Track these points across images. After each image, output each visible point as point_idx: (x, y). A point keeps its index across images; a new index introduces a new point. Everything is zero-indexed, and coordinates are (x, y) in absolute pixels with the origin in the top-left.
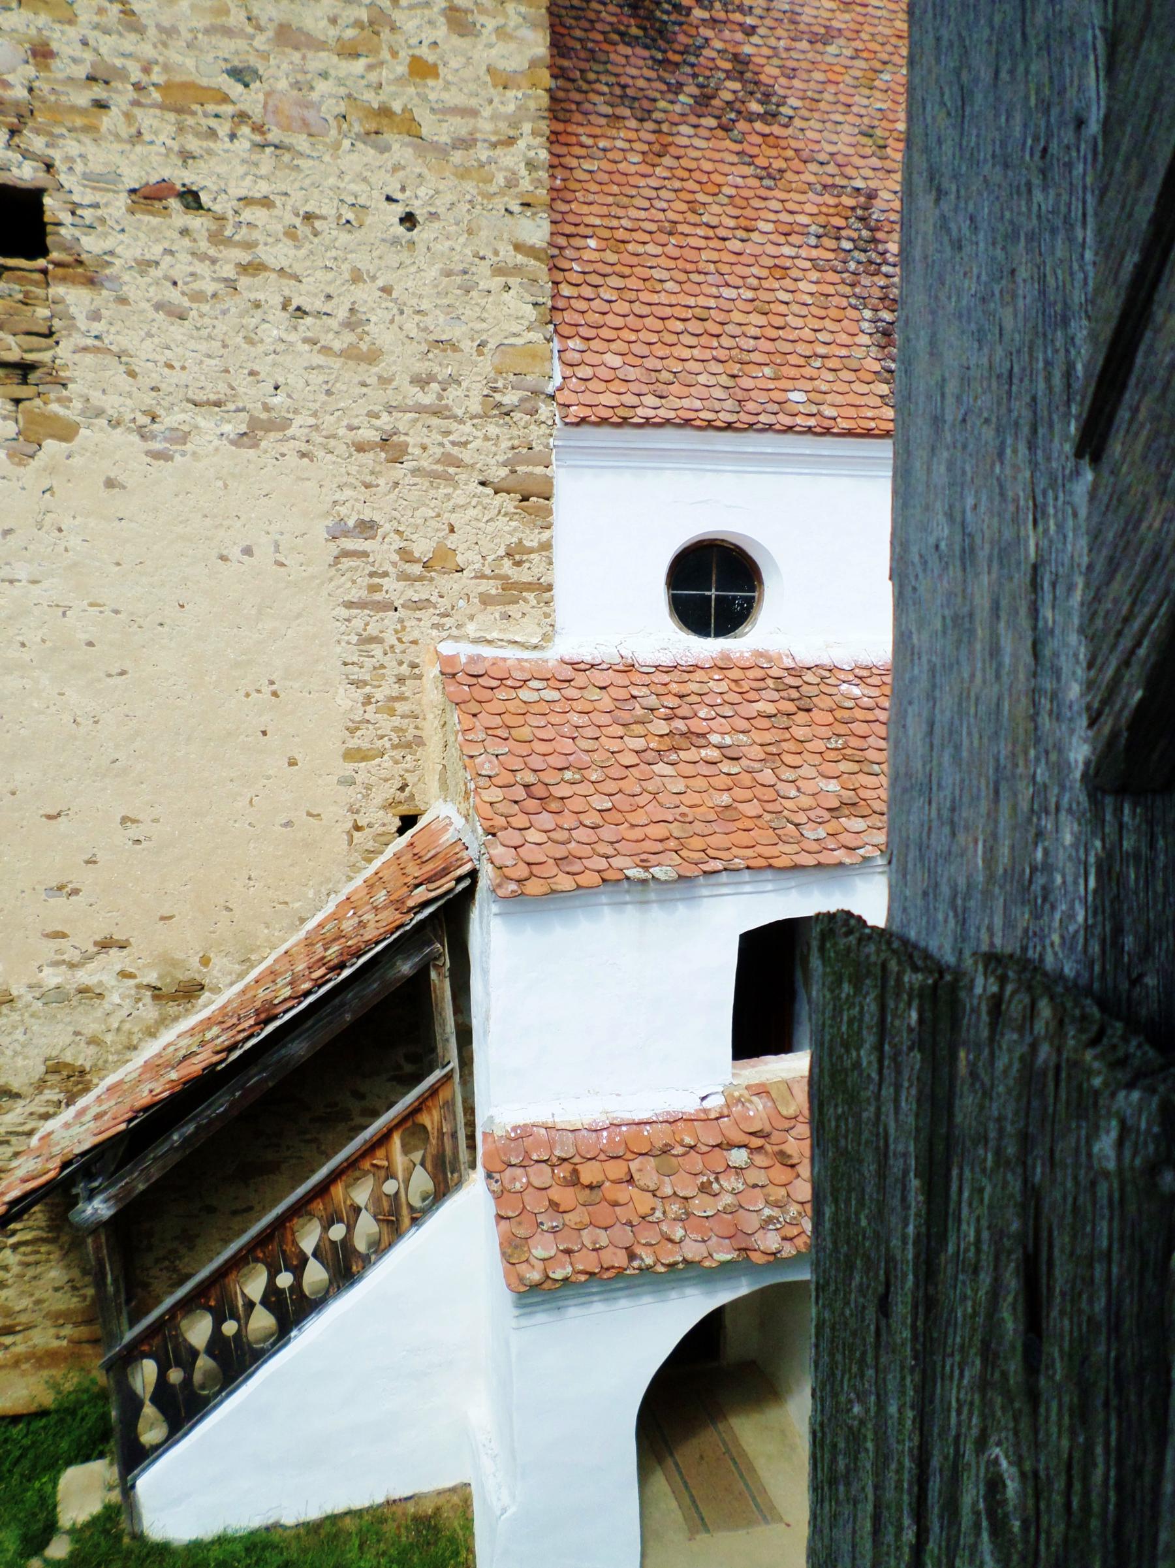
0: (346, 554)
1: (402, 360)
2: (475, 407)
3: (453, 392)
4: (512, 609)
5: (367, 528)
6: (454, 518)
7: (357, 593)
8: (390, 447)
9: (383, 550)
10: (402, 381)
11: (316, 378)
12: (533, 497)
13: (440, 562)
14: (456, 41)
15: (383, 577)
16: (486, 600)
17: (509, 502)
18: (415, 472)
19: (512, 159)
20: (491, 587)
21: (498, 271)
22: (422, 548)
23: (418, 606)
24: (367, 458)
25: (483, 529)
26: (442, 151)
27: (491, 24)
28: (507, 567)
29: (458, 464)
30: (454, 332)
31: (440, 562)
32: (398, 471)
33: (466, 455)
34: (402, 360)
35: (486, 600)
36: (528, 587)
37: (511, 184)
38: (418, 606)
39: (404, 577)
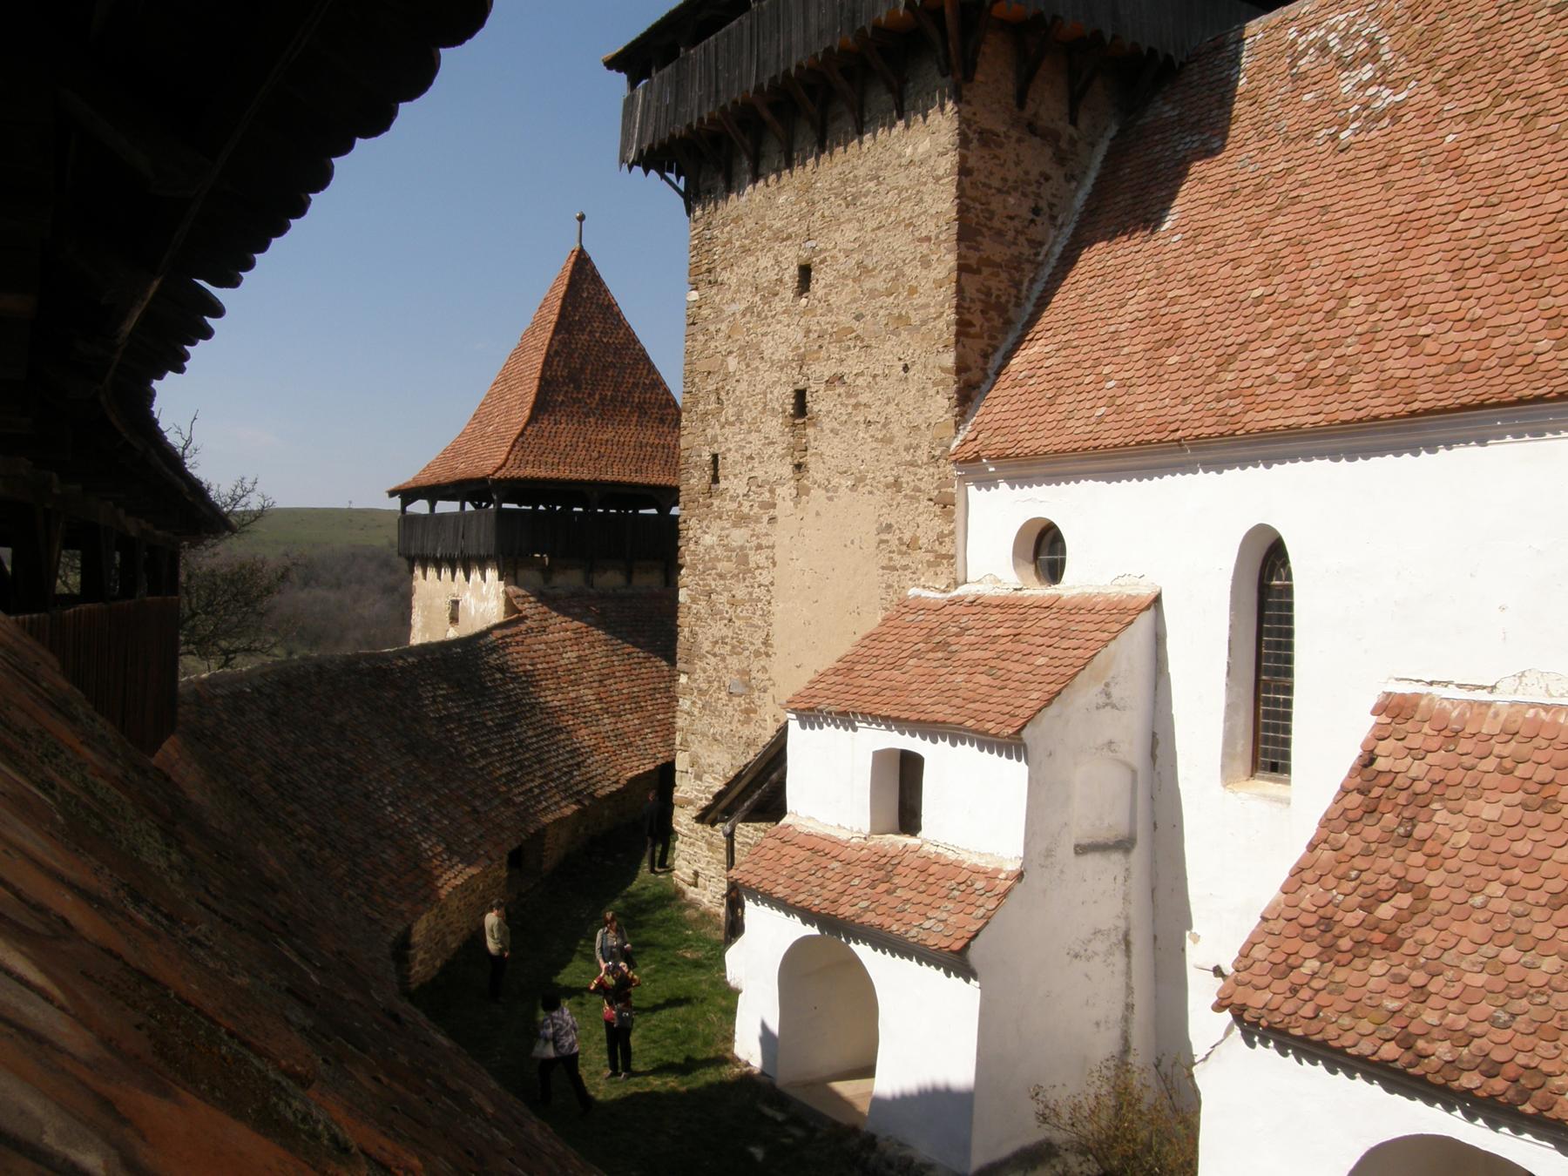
0: (882, 541)
1: (901, 440)
2: (925, 459)
3: (919, 452)
4: (938, 570)
5: (889, 526)
6: (920, 520)
7: (885, 563)
8: (897, 484)
9: (893, 539)
10: (901, 450)
11: (874, 454)
12: (946, 505)
13: (912, 545)
14: (924, 272)
15: (898, 550)
16: (929, 564)
17: (937, 509)
18: (906, 496)
19: (941, 324)
20: (930, 557)
21: (935, 384)
22: (907, 537)
23: (905, 568)
24: (889, 491)
25: (928, 524)
26: (917, 329)
27: (934, 257)
28: (937, 546)
29: (919, 490)
30: (919, 421)
31: (912, 545)
32: (900, 497)
33: (922, 485)
34: (901, 440)
35: (929, 564)
36: (944, 556)
37: (940, 336)
38: (905, 568)
39: (900, 553)
